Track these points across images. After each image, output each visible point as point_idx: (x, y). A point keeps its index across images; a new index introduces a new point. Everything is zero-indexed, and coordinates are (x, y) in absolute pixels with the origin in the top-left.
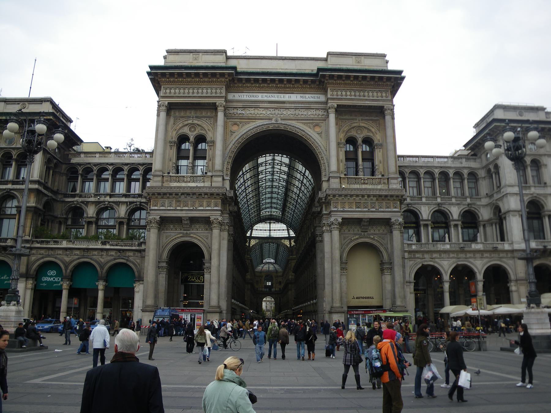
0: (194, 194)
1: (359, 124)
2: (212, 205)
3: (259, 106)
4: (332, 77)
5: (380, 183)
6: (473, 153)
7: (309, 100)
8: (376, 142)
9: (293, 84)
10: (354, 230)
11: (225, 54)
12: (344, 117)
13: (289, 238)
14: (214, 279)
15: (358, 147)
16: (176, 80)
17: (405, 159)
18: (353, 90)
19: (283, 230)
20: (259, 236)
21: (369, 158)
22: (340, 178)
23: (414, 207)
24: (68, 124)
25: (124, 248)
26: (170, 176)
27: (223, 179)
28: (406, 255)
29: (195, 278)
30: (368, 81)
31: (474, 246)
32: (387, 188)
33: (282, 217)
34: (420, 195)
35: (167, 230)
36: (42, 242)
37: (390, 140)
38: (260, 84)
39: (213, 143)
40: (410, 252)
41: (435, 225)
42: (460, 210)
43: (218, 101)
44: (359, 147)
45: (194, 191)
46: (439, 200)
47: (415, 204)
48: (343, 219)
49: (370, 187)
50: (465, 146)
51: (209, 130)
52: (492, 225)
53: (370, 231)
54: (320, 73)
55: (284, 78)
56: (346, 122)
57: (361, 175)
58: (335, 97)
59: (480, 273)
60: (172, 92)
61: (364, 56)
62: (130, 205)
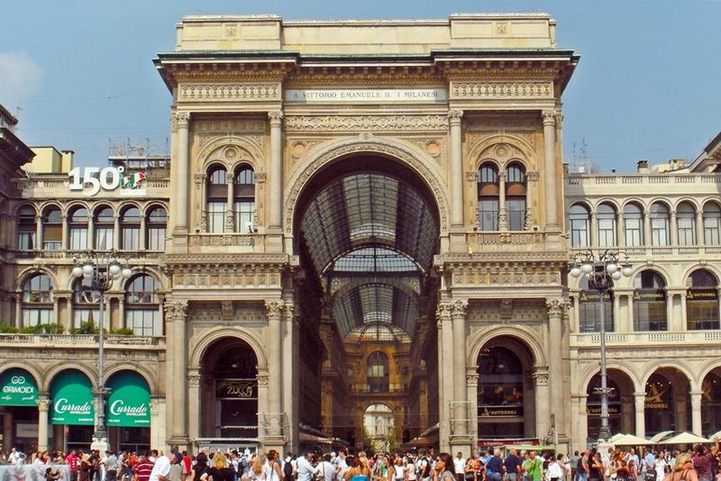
0: (239, 265)
5: (529, 242)
7: (419, 99)
9: (392, 75)
12: (477, 129)
20: (351, 270)
22: (467, 234)
26: (201, 236)
27: (284, 238)
28: (574, 354)
29: (238, 390)
30: (515, 69)
33: (396, 243)
44: (501, 179)
45: (240, 260)
50: (708, 149)
54: (436, 60)
59: (696, 381)
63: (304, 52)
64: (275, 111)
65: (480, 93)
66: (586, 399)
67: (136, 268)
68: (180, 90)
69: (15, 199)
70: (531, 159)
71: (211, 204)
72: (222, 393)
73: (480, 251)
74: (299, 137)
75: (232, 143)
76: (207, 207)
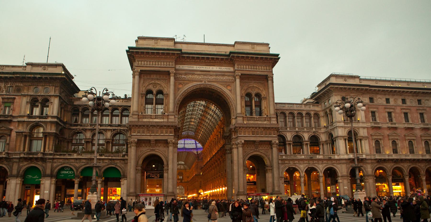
0: (158, 126)
1: (253, 85)
2: (169, 132)
3: (195, 73)
4: (238, 57)
5: (265, 120)
6: (316, 101)
8: (263, 96)
10: (250, 147)
11: (174, 41)
12: (244, 81)
13: (197, 149)
14: (170, 177)
15: (252, 99)
16: (145, 56)
17: (277, 105)
19: (193, 144)
21: (259, 105)
22: (243, 117)
23: (283, 134)
25: (113, 158)
28: (280, 162)
29: (154, 176)
31: (318, 157)
34: (286, 126)
35: (141, 147)
36: (61, 155)
37: (271, 95)
38: (195, 60)
39: (168, 95)
40: (282, 160)
42: (309, 135)
43: (170, 70)
44: (253, 99)
45: (158, 124)
46: (297, 129)
47: (283, 131)
48: (245, 141)
49: (260, 122)
52: (327, 144)
57: (254, 116)
58: (240, 69)
60: (142, 63)
62: (113, 131)
64: (172, 71)
65: (246, 68)
66: (284, 178)
67: (117, 130)
69: (70, 105)
70: (264, 92)
71: (146, 105)
74: (181, 81)
76: (145, 106)
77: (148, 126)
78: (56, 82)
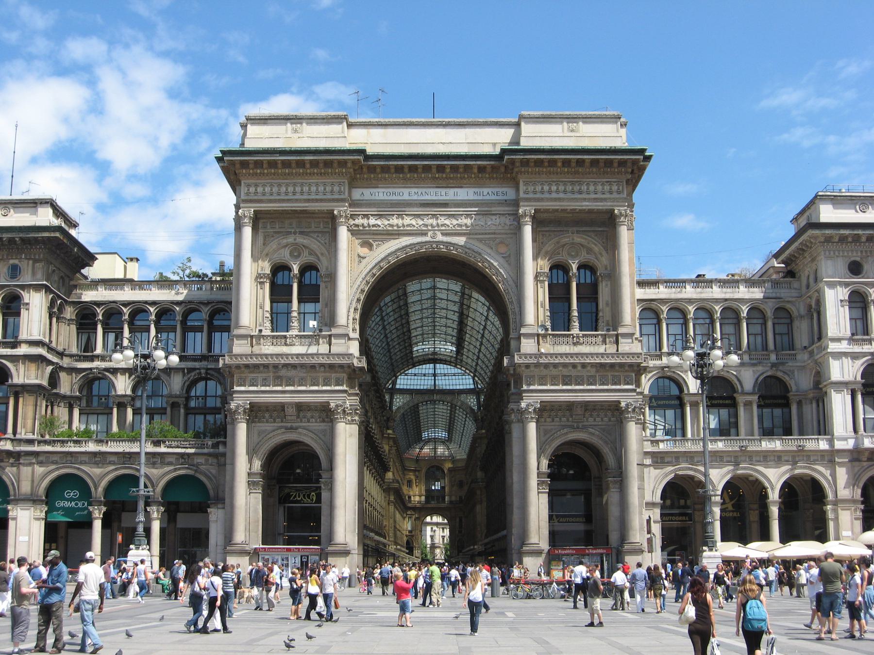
1: (573, 239)
4: (525, 163)
7: (488, 197)
12: (547, 229)
18: (562, 182)
20: (412, 387)
24: (73, 232)
32: (614, 351)
33: (456, 358)
41: (713, 402)
45: (305, 361)
51: (322, 254)
53: (587, 421)
55: (445, 163)
56: (550, 235)
61: (583, 118)
62: (188, 373)
63: (370, 150)
68: (243, 189)
72: (284, 499)
73: (552, 352)
75: (297, 241)
77: (277, 367)
78: (36, 248)
